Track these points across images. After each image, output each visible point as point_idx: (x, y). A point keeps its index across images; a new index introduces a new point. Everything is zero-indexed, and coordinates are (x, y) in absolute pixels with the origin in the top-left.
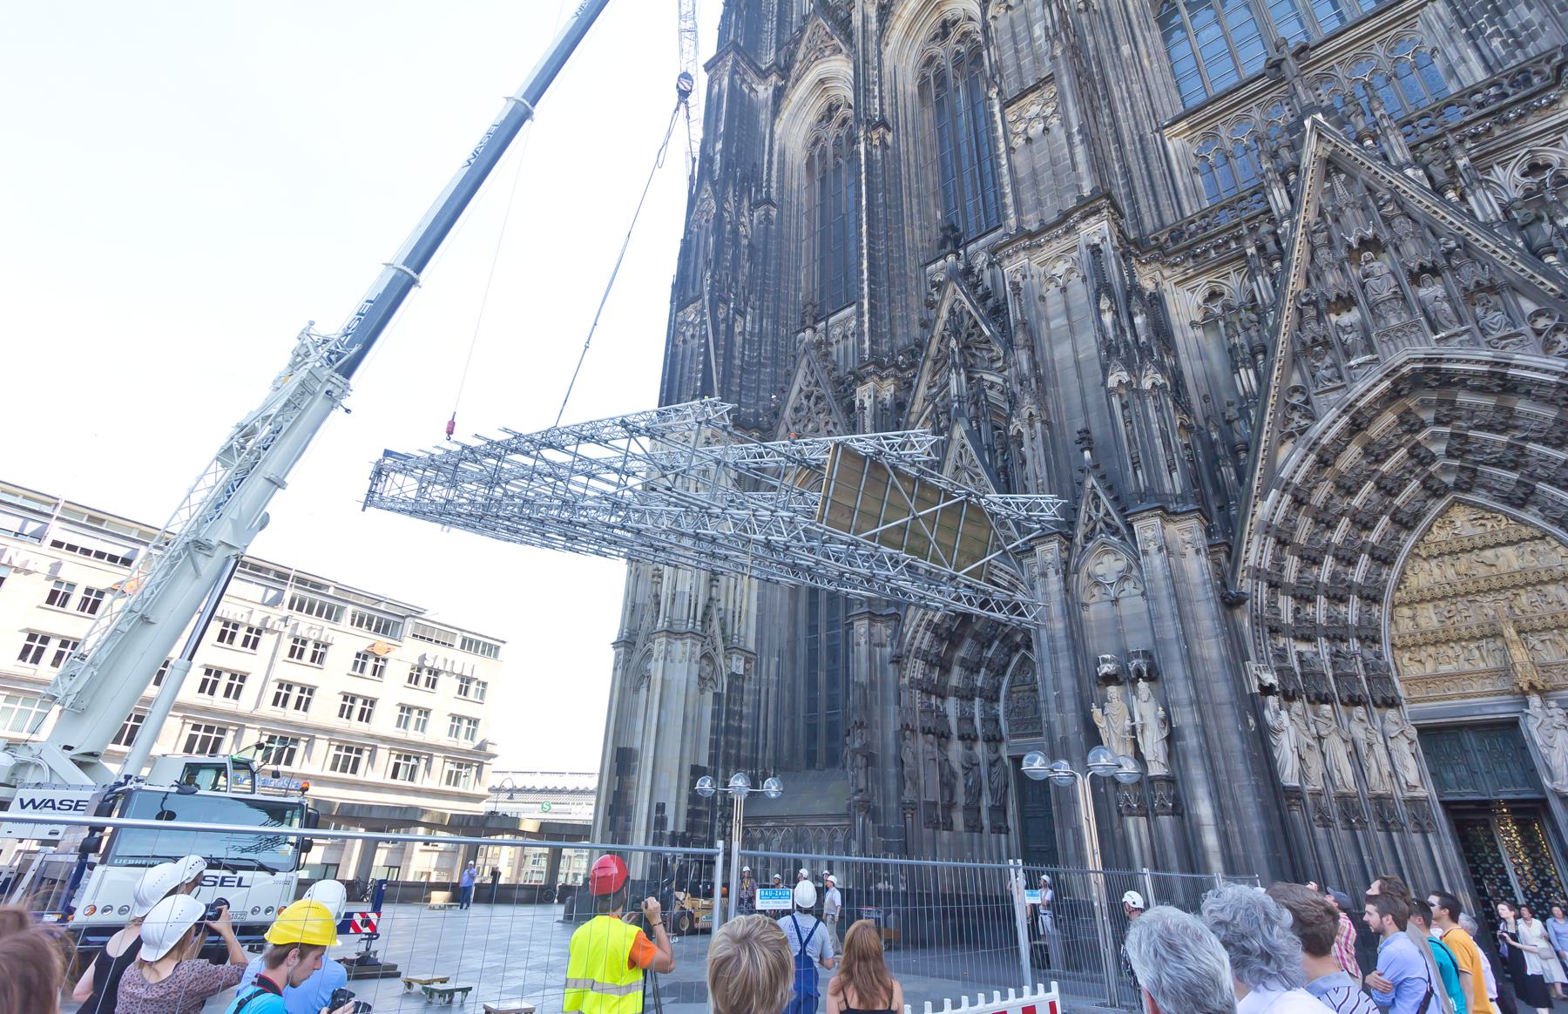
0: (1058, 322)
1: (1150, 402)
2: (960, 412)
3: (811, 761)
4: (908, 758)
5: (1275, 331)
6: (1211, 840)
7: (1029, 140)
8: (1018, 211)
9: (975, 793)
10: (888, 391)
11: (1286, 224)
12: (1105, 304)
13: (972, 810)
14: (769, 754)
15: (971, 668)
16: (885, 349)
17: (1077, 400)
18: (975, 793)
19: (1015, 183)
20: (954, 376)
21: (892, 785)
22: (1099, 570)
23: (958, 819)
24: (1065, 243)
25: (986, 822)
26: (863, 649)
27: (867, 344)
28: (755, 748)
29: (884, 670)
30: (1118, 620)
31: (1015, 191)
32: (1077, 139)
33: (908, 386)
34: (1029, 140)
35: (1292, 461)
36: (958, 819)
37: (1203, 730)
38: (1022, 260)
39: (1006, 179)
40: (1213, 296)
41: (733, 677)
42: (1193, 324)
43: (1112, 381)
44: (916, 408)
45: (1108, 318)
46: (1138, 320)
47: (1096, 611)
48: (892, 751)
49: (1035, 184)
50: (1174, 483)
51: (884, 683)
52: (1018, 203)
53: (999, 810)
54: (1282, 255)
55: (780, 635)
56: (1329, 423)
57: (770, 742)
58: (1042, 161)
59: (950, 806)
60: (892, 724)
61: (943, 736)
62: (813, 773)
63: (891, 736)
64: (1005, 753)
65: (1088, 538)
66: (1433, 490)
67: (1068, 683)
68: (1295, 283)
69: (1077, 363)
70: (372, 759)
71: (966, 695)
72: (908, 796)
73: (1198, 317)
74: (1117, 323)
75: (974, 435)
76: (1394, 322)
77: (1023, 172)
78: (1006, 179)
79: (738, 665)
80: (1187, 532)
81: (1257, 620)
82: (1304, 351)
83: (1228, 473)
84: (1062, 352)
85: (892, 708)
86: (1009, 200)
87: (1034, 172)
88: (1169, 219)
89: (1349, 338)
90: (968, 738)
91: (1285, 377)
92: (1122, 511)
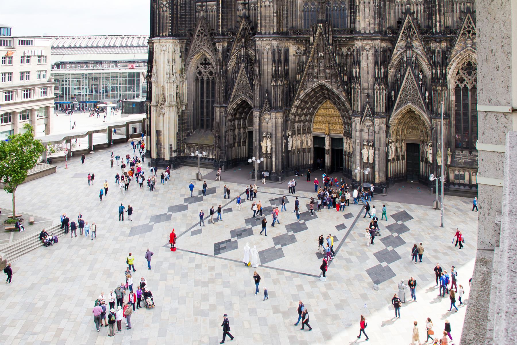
0: (265, 60)
1: (278, 87)
2: (243, 61)
3: (202, 126)
4: (227, 137)
5: (304, 69)
6: (274, 163)
7: (265, 6)
8: (261, 27)
9: (240, 139)
10: (226, 45)
11: (311, 47)
12: (274, 65)
13: (239, 143)
14: (192, 127)
15: (241, 113)
16: (225, 30)
17: (266, 80)
18: (240, 139)
19: (261, 17)
20: (242, 50)
21: (224, 141)
22: (266, 117)
23: (236, 145)
24: (269, 42)
25: (242, 144)
26: (218, 114)
27: (220, 29)
28: (188, 126)
29: (222, 118)
30: (268, 127)
31: (261, 20)
32: (275, 14)
33: (230, 44)
34: (265, 6)
35: (302, 96)
36: (236, 145)
37: (276, 149)
38: (260, 42)
39: (259, 15)
40: (298, 49)
41: (183, 111)
42: (294, 55)
43: (272, 84)
44: (233, 51)
45: (274, 68)
46: (280, 68)
47: (264, 124)
48: (224, 135)
49: (265, 20)
50: (279, 104)
51: (222, 121)
52: (261, 23)
53: (244, 142)
54: (309, 52)
55: (193, 98)
56: (308, 90)
57: (192, 124)
58: (268, 14)
59: (234, 143)
60: (224, 129)
61: (234, 130)
62: (203, 131)
63: (224, 132)
64: (247, 131)
65: (264, 111)
66: (325, 98)
67: (258, 137)
68: (310, 60)
69: (268, 72)
70: (17, 93)
71: (239, 119)
72: (227, 144)
73: (295, 54)
74: (275, 70)
75: (246, 68)
76: (322, 75)
77: (263, 14)
78: (259, 15)
79: (184, 108)
80: (280, 115)
81: (291, 122)
82: (308, 75)
83: (292, 95)
84: (265, 67)
85: (224, 126)
86: (259, 22)
87: (265, 16)
88: (294, 25)
89: (315, 75)
90: (239, 129)
91: (304, 79)
92: (271, 109)
